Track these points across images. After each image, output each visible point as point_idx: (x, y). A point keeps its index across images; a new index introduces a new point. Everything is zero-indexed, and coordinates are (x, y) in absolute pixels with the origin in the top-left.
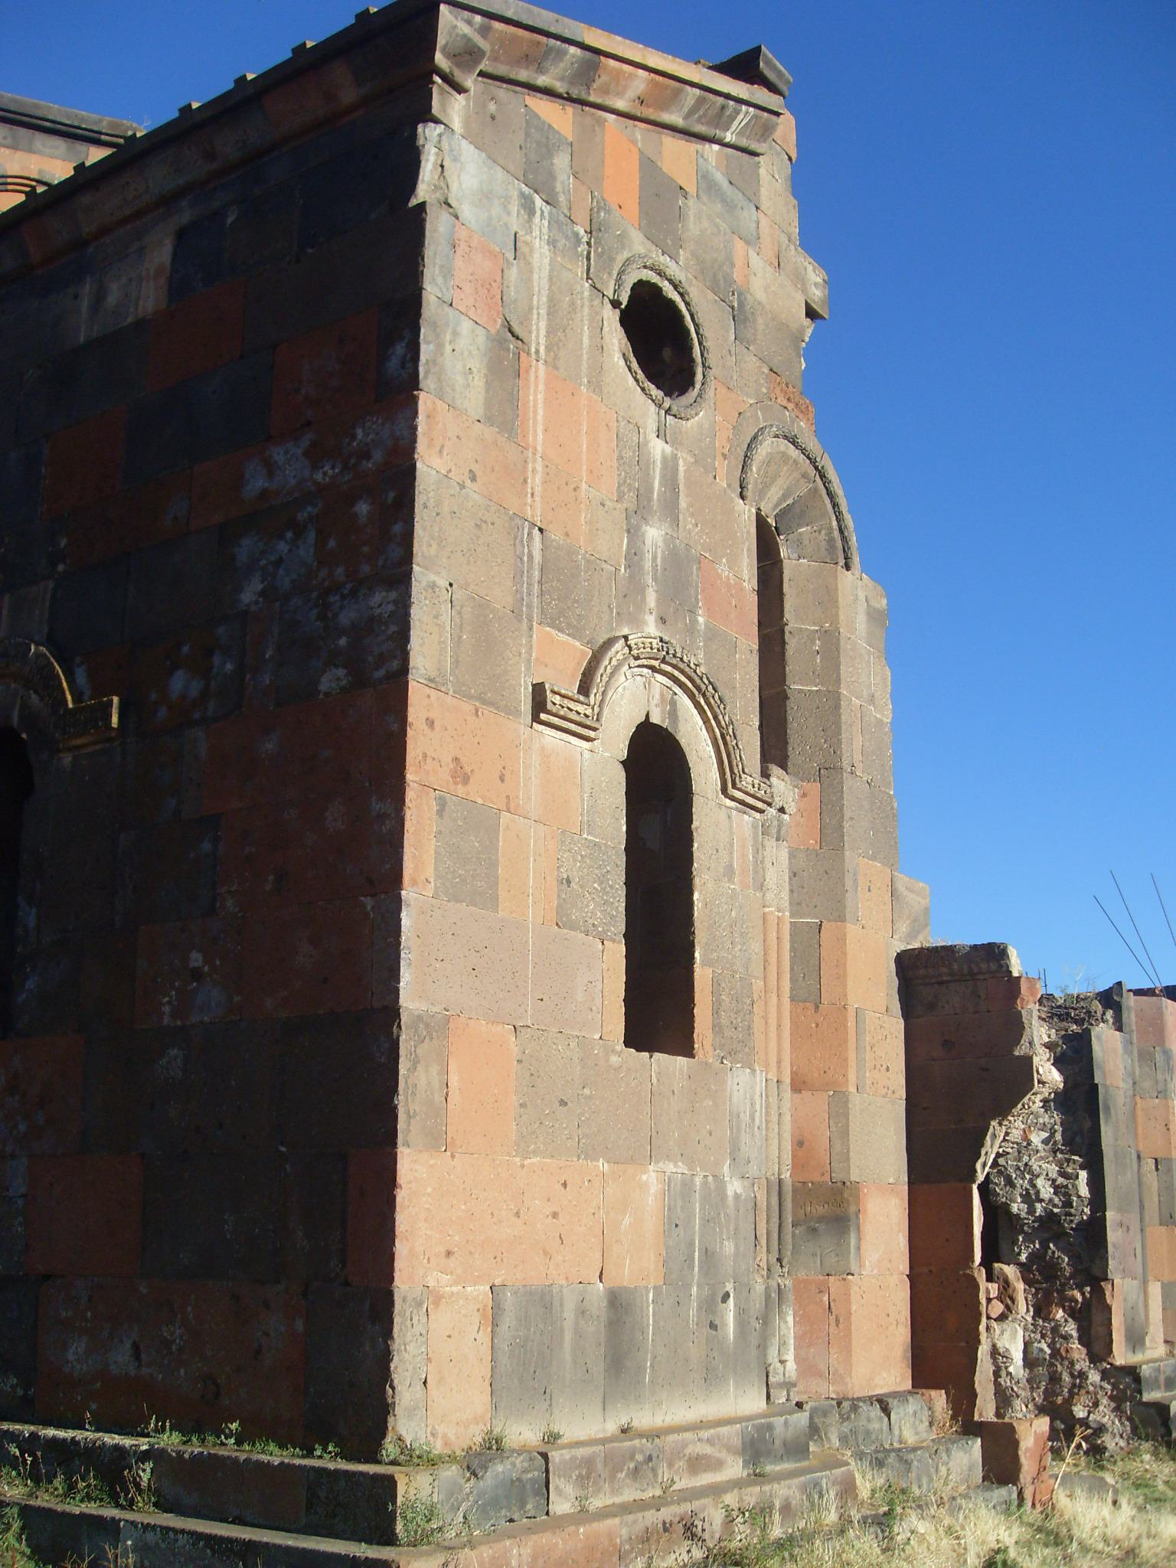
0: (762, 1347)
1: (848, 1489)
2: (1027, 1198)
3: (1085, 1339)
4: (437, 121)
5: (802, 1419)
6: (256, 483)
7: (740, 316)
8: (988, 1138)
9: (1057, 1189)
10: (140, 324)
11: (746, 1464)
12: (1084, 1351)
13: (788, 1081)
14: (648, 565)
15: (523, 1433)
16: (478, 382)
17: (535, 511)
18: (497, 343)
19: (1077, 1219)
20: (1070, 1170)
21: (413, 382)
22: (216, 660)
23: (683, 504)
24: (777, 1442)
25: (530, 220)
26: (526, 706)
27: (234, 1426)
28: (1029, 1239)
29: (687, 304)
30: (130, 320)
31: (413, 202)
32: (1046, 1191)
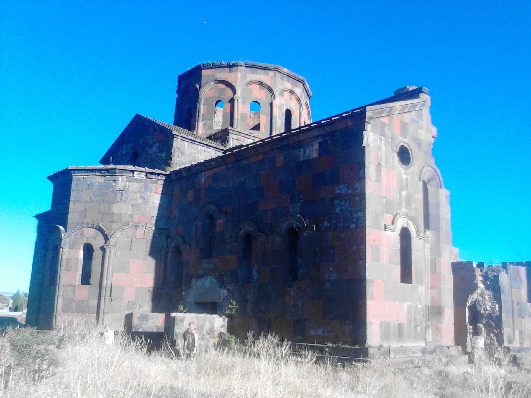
0: (425, 335)
1: (440, 360)
2: (484, 310)
3: (498, 340)
4: (366, 130)
5: (432, 348)
6: (338, 191)
7: (419, 145)
8: (469, 298)
9: (491, 308)
10: (313, 159)
11: (422, 354)
12: (497, 343)
13: (429, 287)
14: (403, 199)
15: (386, 345)
16: (374, 175)
17: (384, 195)
18: (377, 166)
19: (496, 315)
20: (494, 304)
21: (365, 178)
22: (332, 221)
23: (409, 186)
24: (427, 351)
25: (381, 142)
26: (383, 227)
27: (341, 343)
28: (485, 319)
29: (409, 147)
30: (311, 158)
31: (363, 145)
32: (489, 308)
